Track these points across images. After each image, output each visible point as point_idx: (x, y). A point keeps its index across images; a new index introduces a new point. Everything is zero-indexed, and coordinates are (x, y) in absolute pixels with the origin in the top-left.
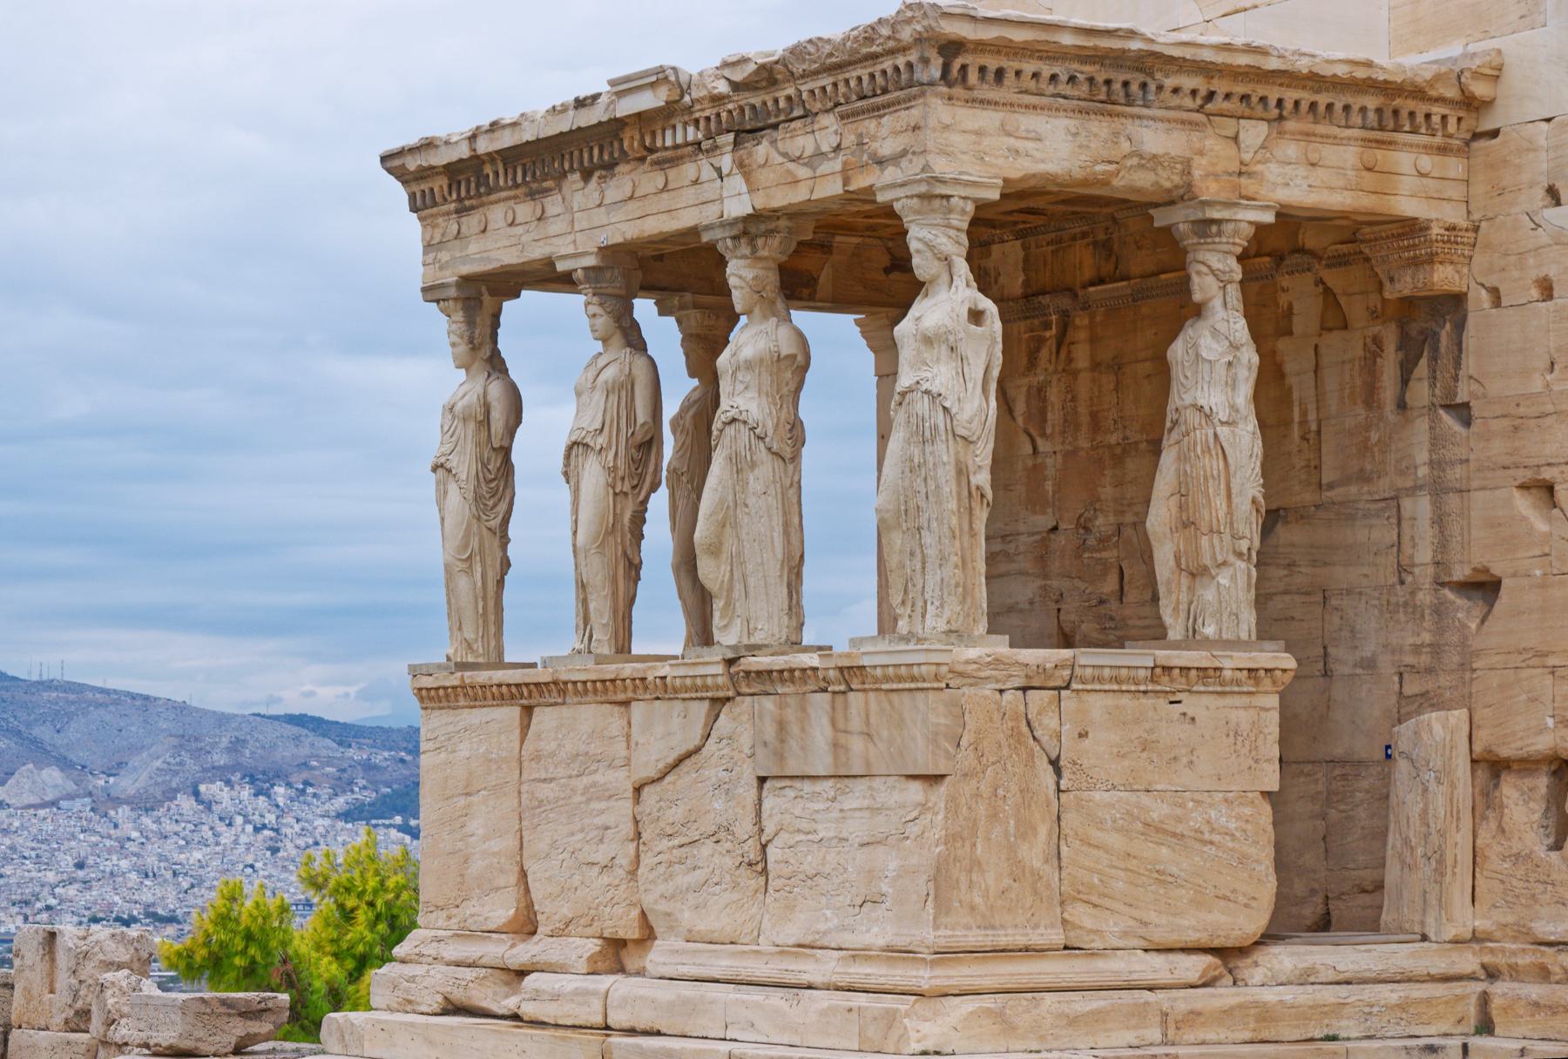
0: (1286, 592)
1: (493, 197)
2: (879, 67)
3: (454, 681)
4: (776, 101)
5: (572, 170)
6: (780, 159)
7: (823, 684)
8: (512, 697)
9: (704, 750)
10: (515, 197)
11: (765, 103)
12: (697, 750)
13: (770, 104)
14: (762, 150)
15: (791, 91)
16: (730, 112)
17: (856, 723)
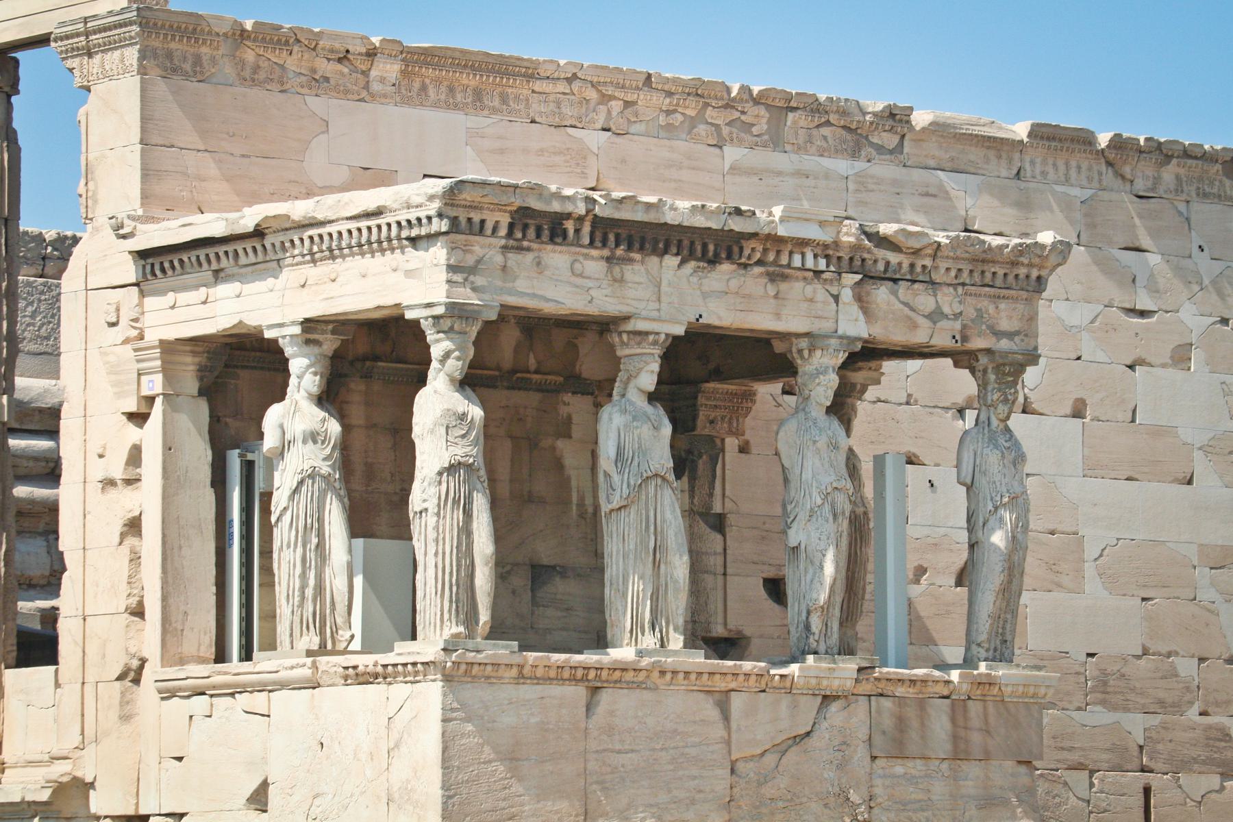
0: (563, 629)
1: (558, 248)
2: (1016, 271)
3: (516, 659)
4: (912, 266)
5: (677, 254)
6: (901, 306)
7: (946, 693)
8: (582, 680)
9: (815, 735)
10: (586, 256)
11: (900, 264)
12: (808, 734)
13: (905, 266)
14: (881, 294)
15: (928, 262)
16: (863, 260)
17: (975, 722)
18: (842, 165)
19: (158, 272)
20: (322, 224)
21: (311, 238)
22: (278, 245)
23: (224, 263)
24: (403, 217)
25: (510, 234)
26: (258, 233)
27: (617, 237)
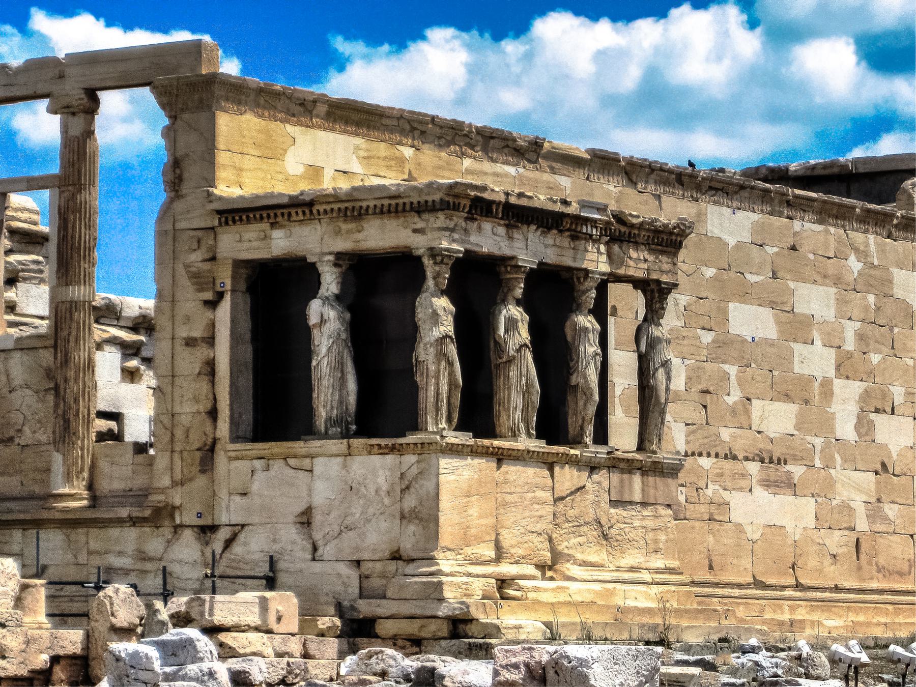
3: (472, 442)
4: (630, 233)
10: (499, 224)
12: (584, 487)
14: (616, 248)
15: (636, 232)
18: (512, 170)
19: (230, 223)
20: (356, 200)
21: (346, 208)
22: (322, 211)
23: (280, 219)
24: (415, 200)
25: (469, 212)
26: (310, 204)
27: (513, 213)
